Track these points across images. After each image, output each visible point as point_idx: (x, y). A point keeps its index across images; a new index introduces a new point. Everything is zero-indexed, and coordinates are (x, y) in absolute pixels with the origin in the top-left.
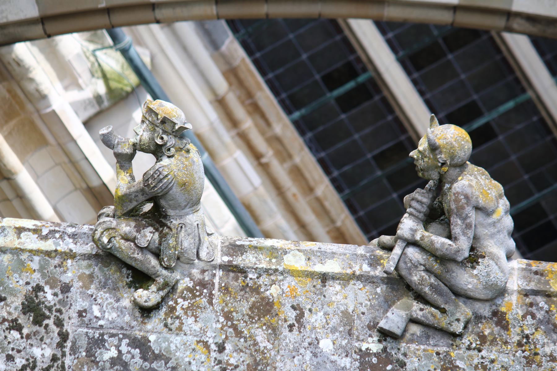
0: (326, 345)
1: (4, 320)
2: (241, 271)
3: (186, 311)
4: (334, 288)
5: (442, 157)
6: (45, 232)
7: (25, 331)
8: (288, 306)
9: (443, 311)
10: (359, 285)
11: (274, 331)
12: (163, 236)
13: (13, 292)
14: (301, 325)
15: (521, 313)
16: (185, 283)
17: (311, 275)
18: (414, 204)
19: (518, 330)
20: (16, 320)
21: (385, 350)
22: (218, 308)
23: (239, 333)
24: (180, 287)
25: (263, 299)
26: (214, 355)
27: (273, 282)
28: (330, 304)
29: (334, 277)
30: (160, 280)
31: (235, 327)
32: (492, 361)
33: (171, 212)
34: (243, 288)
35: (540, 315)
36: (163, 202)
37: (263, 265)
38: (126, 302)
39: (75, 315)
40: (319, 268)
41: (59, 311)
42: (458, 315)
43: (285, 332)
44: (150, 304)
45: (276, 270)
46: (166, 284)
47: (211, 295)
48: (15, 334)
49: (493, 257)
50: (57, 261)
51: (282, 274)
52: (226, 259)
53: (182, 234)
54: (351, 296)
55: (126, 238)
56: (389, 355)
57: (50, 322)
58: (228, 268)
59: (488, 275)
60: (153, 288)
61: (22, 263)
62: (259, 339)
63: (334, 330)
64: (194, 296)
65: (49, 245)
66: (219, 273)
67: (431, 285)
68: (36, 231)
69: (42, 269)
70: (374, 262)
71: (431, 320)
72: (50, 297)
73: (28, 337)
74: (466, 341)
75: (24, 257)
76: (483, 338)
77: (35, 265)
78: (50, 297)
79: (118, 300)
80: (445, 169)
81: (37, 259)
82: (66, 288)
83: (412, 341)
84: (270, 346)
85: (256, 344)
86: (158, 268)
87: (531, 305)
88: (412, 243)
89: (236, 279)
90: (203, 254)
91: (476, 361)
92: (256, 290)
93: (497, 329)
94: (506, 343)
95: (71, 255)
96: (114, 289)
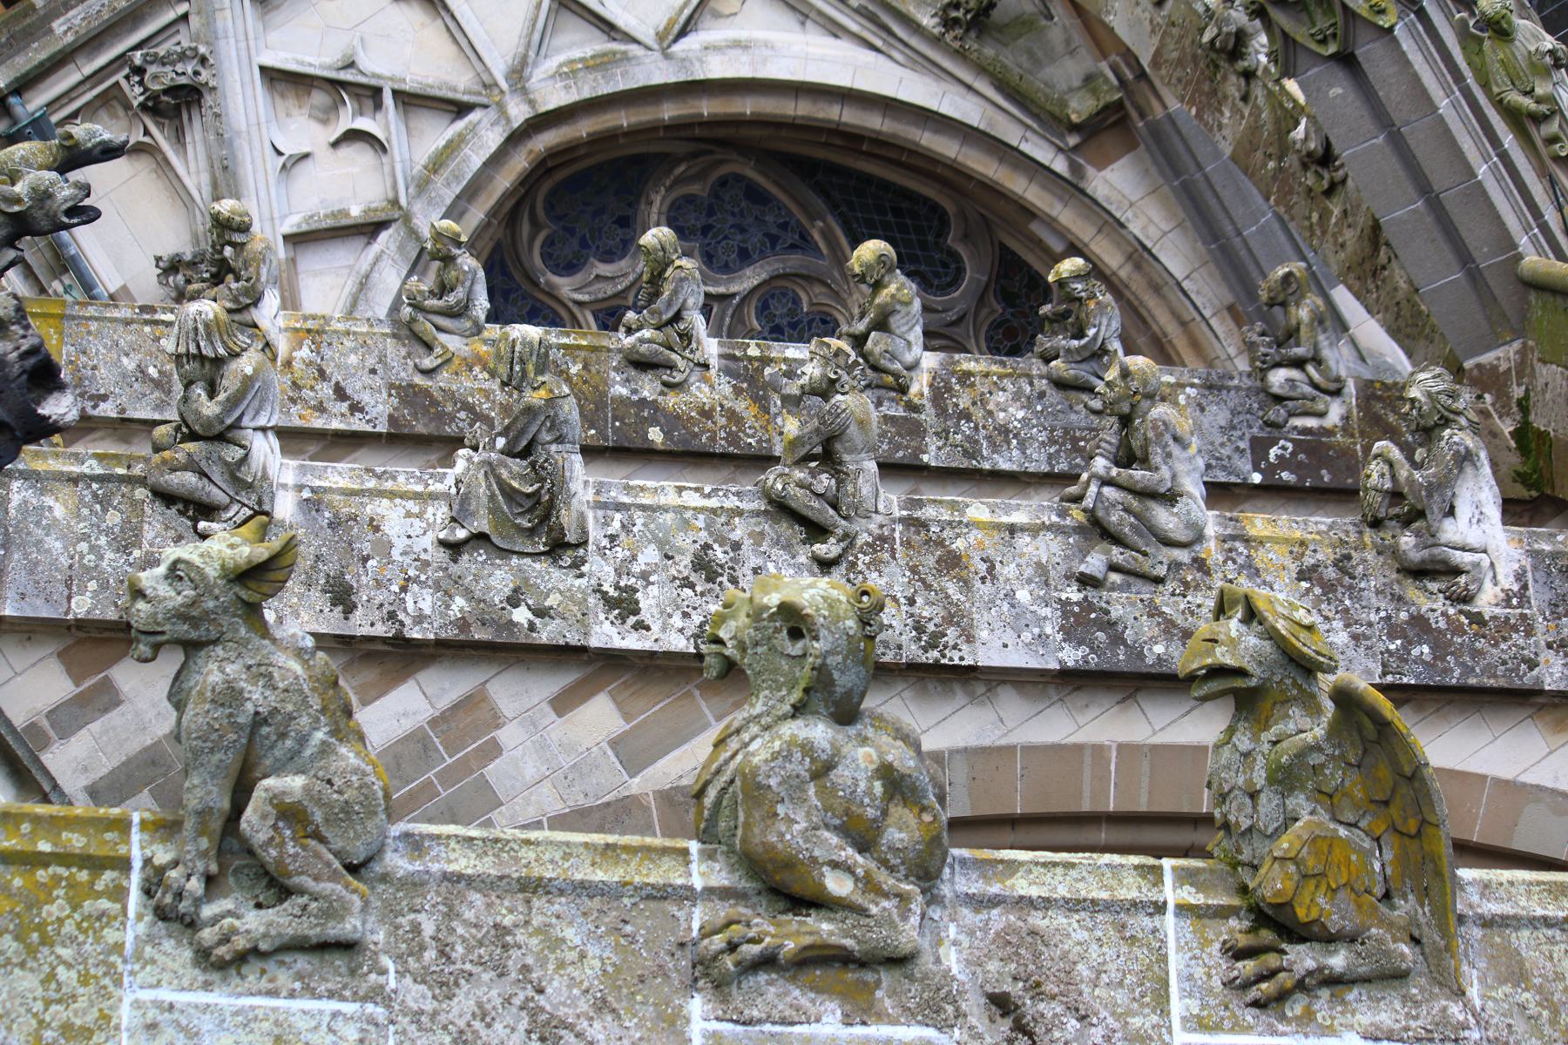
0: (1023, 595)
1: (675, 578)
2: (922, 525)
3: (868, 566)
4: (1023, 540)
5: (1134, 385)
6: (707, 490)
7: (699, 589)
8: (977, 559)
9: (1145, 554)
10: (1050, 536)
11: (966, 585)
12: (840, 482)
13: (681, 551)
14: (994, 578)
15: (1221, 559)
16: (864, 538)
17: (998, 527)
18: (1103, 444)
19: (1220, 575)
20: (687, 578)
21: (1086, 598)
22: (902, 563)
23: (928, 587)
24: (859, 542)
25: (949, 552)
26: (904, 608)
27: (958, 536)
28: (1021, 555)
29: (1023, 529)
30: (839, 531)
31: (923, 581)
32: (1199, 606)
33: (846, 457)
34: (927, 542)
35: (1240, 560)
36: (838, 446)
37: (946, 517)
38: (802, 559)
39: (749, 572)
40: (1005, 519)
41: (732, 568)
42: (1160, 558)
43: (978, 584)
44: (831, 556)
45: (960, 522)
46: (846, 536)
47: (893, 551)
48: (688, 592)
49: (1191, 496)
50: (723, 519)
51: (967, 526)
52: (905, 513)
53: (861, 480)
54: (1043, 547)
55: (801, 485)
56: (1090, 604)
57: (724, 579)
58: (909, 522)
59: (1189, 513)
60: (832, 540)
61: (686, 522)
62: (950, 592)
63: (1029, 581)
64: (875, 551)
65: (713, 503)
66: (899, 528)
67: (1131, 525)
68: (697, 490)
69: (708, 527)
70: (1063, 514)
71: (1132, 566)
72: (720, 555)
73: (702, 594)
74: (1170, 586)
75: (688, 515)
76: (1186, 585)
77: (700, 523)
78: (720, 555)
79: (793, 557)
80: (1138, 397)
81: (701, 517)
82: (736, 546)
83: (1113, 589)
84: (963, 599)
85: (948, 597)
86: (837, 517)
87: (1230, 550)
88: (1107, 482)
89: (919, 533)
90: (881, 507)
91: (1182, 607)
92: (940, 543)
93: (1199, 575)
94: (1210, 588)
95: (739, 512)
96: (788, 547)
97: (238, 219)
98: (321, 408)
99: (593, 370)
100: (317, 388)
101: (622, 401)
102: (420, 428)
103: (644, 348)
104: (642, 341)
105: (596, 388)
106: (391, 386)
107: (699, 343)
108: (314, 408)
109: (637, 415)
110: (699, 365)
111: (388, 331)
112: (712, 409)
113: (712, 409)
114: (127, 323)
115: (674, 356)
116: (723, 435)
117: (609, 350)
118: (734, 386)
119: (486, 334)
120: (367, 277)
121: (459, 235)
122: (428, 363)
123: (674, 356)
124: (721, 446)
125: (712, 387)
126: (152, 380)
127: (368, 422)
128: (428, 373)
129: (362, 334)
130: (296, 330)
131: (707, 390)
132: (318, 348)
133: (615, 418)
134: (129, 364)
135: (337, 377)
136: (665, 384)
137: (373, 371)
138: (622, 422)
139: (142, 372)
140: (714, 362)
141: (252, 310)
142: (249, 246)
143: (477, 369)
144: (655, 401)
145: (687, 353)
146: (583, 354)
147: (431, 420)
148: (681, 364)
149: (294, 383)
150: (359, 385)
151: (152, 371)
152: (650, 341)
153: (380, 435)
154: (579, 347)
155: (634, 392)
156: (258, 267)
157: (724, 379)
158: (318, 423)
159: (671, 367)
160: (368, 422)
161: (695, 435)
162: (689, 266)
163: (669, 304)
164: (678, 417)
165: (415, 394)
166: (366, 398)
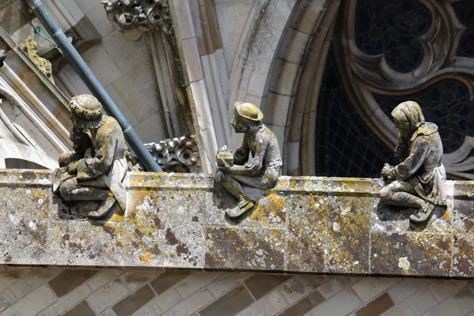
97: (90, 112)
98: (156, 251)
99: (359, 211)
100: (154, 234)
101: (380, 236)
102: (229, 265)
103: (396, 195)
104: (395, 190)
105: (360, 226)
106: (208, 230)
107: (438, 189)
108: (151, 251)
109: (390, 247)
110: (437, 206)
111: (206, 186)
112: (448, 241)
113: (448, 241)
114: (13, 186)
115: (419, 201)
116: (456, 262)
117: (370, 195)
118: (466, 221)
119: (279, 187)
120: (266, 7)
121: (256, 116)
122: (235, 212)
123: (419, 201)
124: (454, 271)
125: (449, 222)
126: (32, 232)
127: (191, 260)
128: (236, 220)
129: (187, 189)
130: (139, 188)
131: (445, 225)
132: (155, 201)
133: (374, 251)
134: (15, 220)
135: (168, 225)
136: (412, 222)
137: (195, 219)
138: (380, 254)
139: (24, 226)
140: (450, 203)
141: (105, 177)
142: (99, 132)
143: (272, 214)
144: (405, 235)
145: (429, 198)
146: (351, 199)
147: (237, 257)
148: (425, 206)
149: (137, 231)
150: (184, 231)
151: (32, 225)
152: (400, 190)
153: (200, 270)
154: (348, 194)
155: (389, 228)
156: (107, 148)
157: (459, 215)
158: (154, 263)
159: (417, 208)
160: (191, 260)
161: (434, 263)
162: (429, 132)
163: (414, 163)
164: (422, 248)
165: (226, 236)
166: (189, 241)
